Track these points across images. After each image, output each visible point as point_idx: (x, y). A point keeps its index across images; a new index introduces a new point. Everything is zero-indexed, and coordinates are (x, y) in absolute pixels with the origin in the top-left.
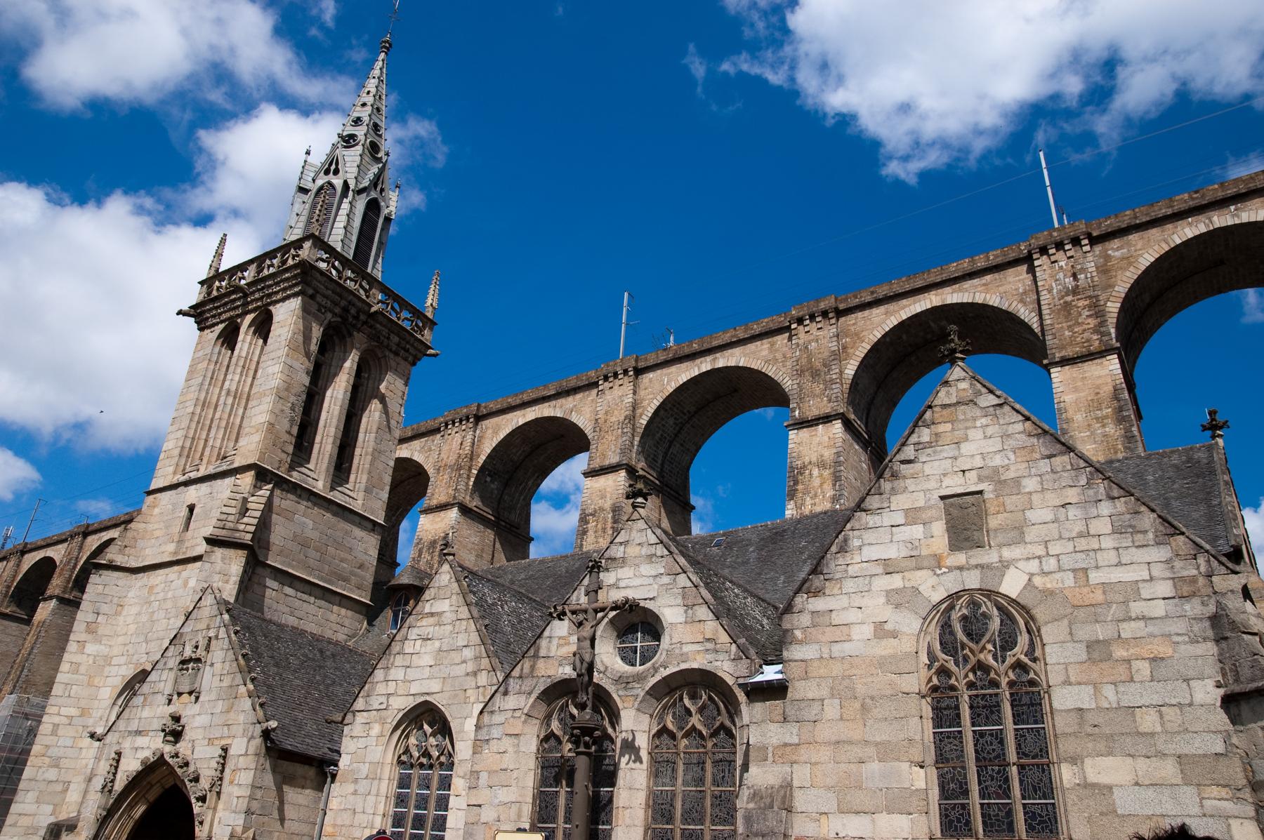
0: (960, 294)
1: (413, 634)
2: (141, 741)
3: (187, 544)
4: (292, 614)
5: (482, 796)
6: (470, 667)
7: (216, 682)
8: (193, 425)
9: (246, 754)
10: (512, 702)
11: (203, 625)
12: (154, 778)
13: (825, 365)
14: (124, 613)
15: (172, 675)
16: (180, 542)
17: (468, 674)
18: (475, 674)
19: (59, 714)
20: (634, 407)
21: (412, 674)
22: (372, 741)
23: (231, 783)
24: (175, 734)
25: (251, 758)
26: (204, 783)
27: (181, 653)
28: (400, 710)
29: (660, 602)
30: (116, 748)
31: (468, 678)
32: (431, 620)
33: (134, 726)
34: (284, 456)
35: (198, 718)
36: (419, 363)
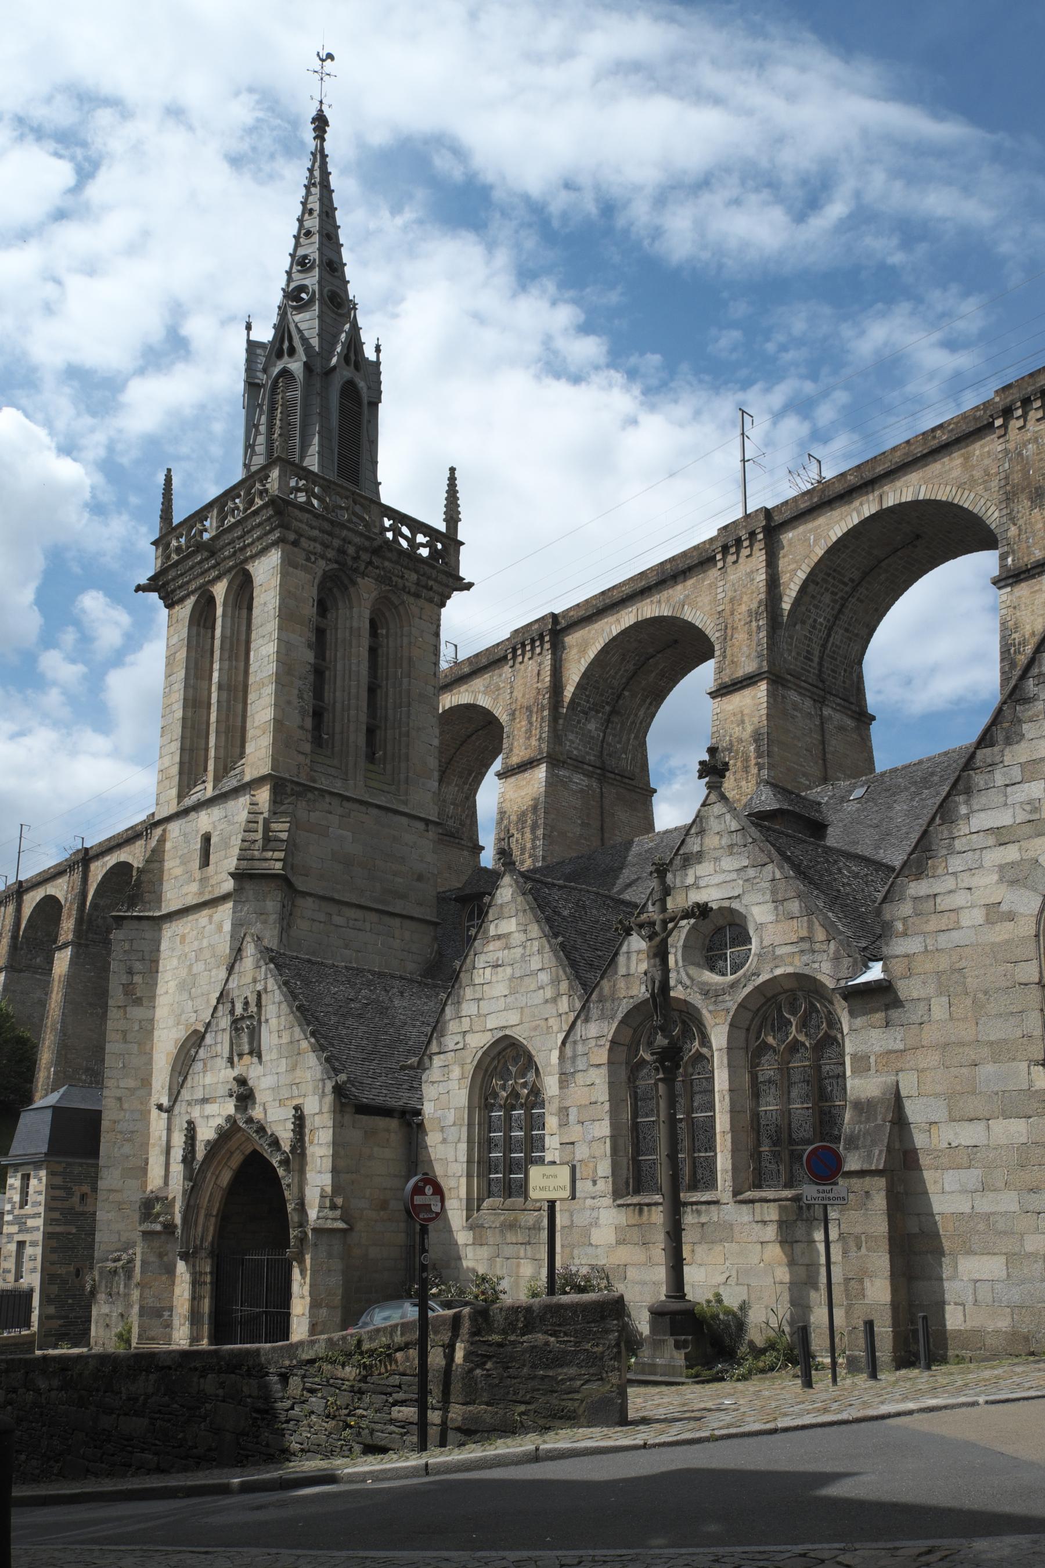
1: (480, 961)
2: (210, 1109)
3: (213, 882)
4: (346, 946)
5: (575, 1132)
6: (549, 993)
7: (275, 1040)
9: (321, 1113)
10: (593, 1029)
11: (248, 979)
12: (232, 1144)
15: (226, 1037)
16: (204, 881)
17: (547, 1001)
18: (554, 1000)
19: (118, 1087)
20: (773, 583)
22: (454, 1085)
25: (326, 1115)
26: (286, 1147)
27: (232, 1012)
29: (747, 899)
30: (187, 1118)
31: (548, 1005)
32: (498, 944)
33: (199, 1095)
34: (301, 758)
35: (263, 1079)
36: (449, 602)
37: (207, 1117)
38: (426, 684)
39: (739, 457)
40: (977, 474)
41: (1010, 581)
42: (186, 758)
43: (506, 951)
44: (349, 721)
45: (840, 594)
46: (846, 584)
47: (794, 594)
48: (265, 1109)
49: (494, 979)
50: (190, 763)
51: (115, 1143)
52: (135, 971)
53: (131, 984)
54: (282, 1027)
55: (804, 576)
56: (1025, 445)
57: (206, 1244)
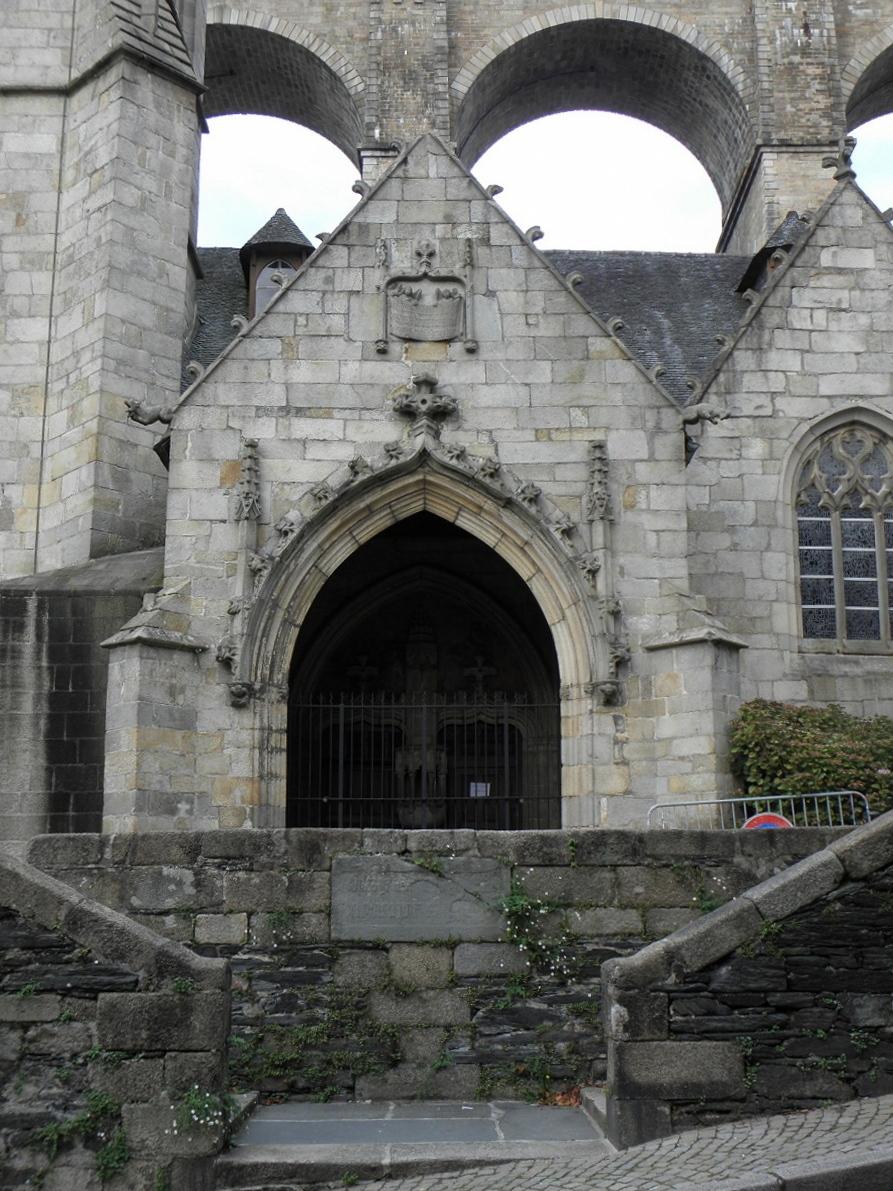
0: (641, 11)
13: (426, 67)
21: (816, 363)
23: (631, 507)
27: (386, 264)
28: (802, 420)
40: (340, 32)
41: (378, 153)
43: (857, 293)
49: (833, 326)
54: (538, 309)
56: (401, 22)
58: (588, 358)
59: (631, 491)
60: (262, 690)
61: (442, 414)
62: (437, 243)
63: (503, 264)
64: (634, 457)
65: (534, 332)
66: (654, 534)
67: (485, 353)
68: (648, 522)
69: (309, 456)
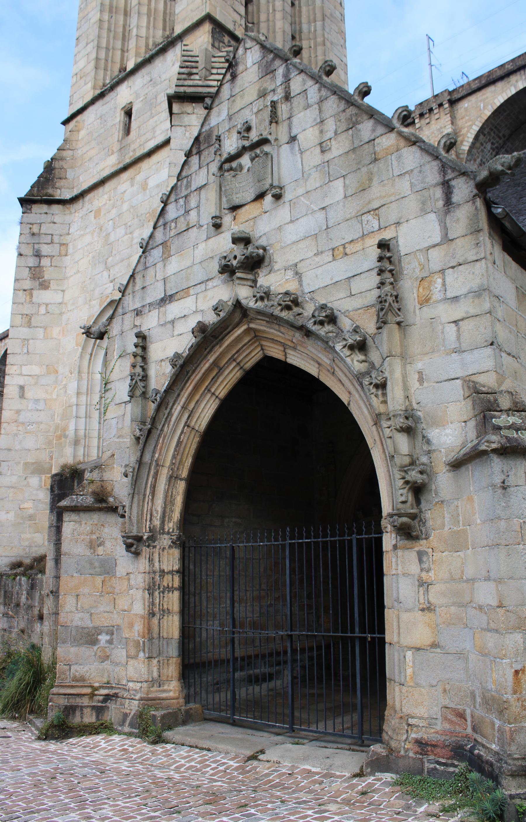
7: (314, 157)
8: (104, 34)
11: (252, 94)
14: (70, 250)
23: (425, 301)
24: (251, 262)
33: (156, 293)
34: (237, 17)
37: (173, 322)
38: (335, 8)
39: (428, 63)
42: (102, 55)
44: (274, 10)
45: (496, 145)
46: (500, 138)
47: (471, 140)
48: (297, 273)
50: (106, 60)
51: (16, 435)
52: (44, 253)
53: (39, 266)
55: (477, 129)
57: (171, 526)
58: (376, 160)
59: (426, 284)
60: (152, 538)
61: (254, 263)
62: (254, 116)
63: (301, 108)
64: (426, 245)
65: (328, 156)
66: (453, 325)
67: (288, 196)
68: (446, 313)
69: (176, 333)
